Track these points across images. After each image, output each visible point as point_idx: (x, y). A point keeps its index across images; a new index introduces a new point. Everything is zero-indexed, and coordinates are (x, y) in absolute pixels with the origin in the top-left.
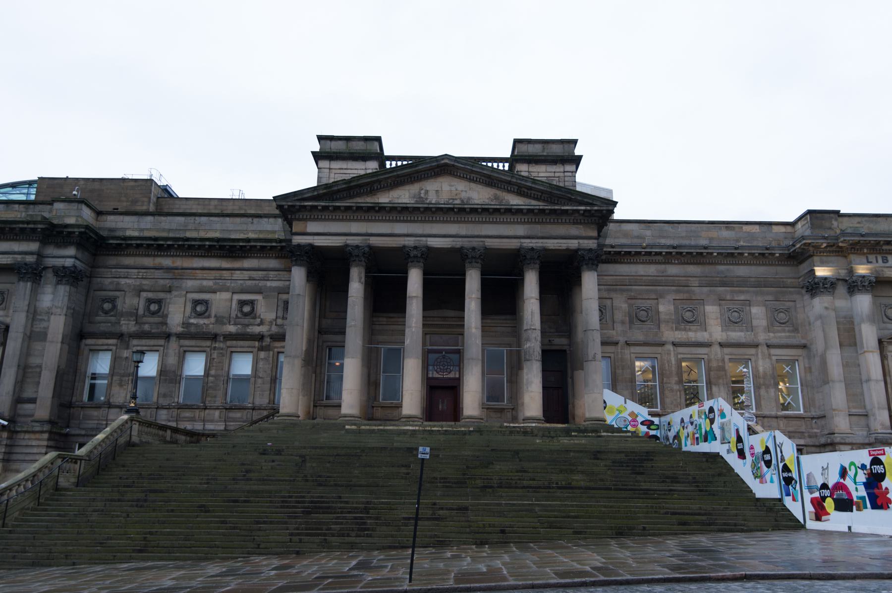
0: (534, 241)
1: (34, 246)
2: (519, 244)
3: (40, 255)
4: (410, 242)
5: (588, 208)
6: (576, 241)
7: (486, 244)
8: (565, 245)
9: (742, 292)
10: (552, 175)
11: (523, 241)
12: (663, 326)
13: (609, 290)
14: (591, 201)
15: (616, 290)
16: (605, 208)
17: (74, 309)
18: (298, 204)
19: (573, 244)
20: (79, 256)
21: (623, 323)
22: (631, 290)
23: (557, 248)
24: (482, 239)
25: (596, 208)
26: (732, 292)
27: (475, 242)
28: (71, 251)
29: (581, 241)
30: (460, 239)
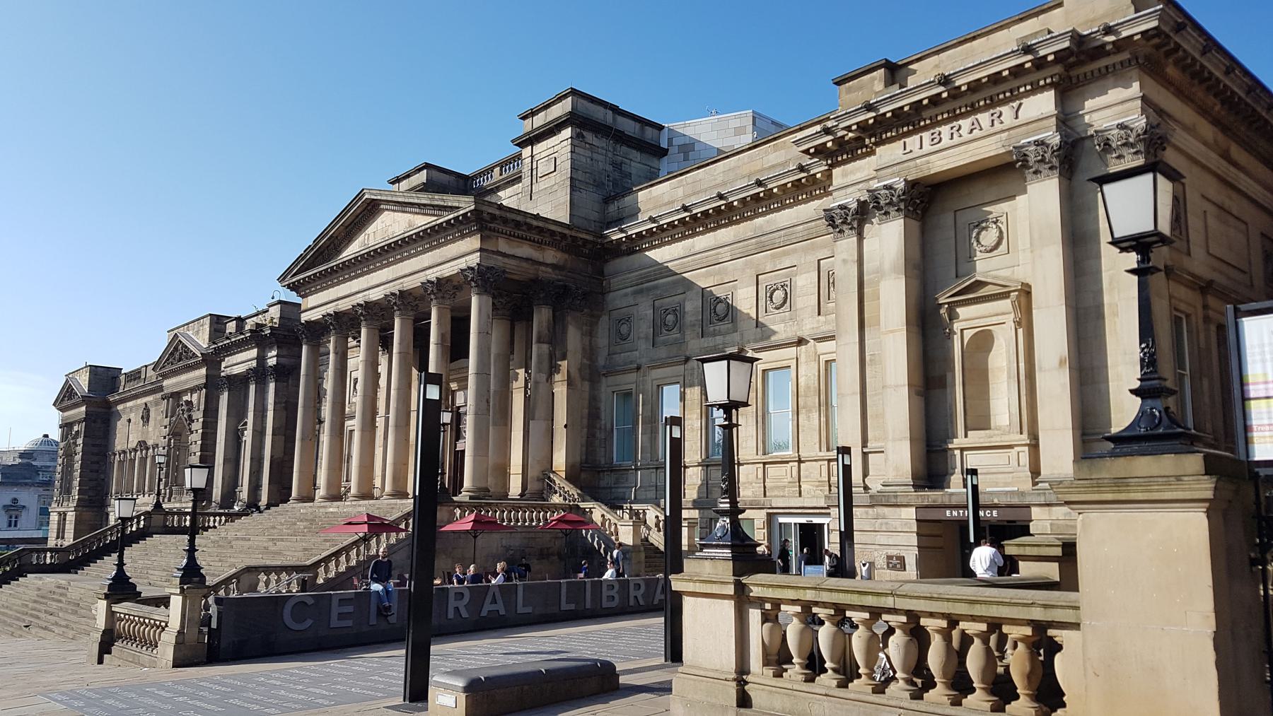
0: (435, 269)
1: (253, 353)
2: (425, 278)
3: (261, 359)
4: (359, 299)
5: (456, 214)
6: (463, 260)
7: (405, 285)
8: (456, 267)
9: (785, 254)
10: (551, 151)
11: (428, 272)
12: (688, 332)
13: (636, 293)
14: (457, 205)
15: (641, 292)
16: (467, 210)
17: (286, 402)
18: (291, 281)
19: (462, 264)
20: (285, 352)
21: (647, 338)
22: (656, 287)
23: (451, 273)
24: (402, 280)
25: (461, 212)
26: (773, 256)
27: (394, 288)
28: (274, 353)
29: (467, 258)
30: (388, 285)
